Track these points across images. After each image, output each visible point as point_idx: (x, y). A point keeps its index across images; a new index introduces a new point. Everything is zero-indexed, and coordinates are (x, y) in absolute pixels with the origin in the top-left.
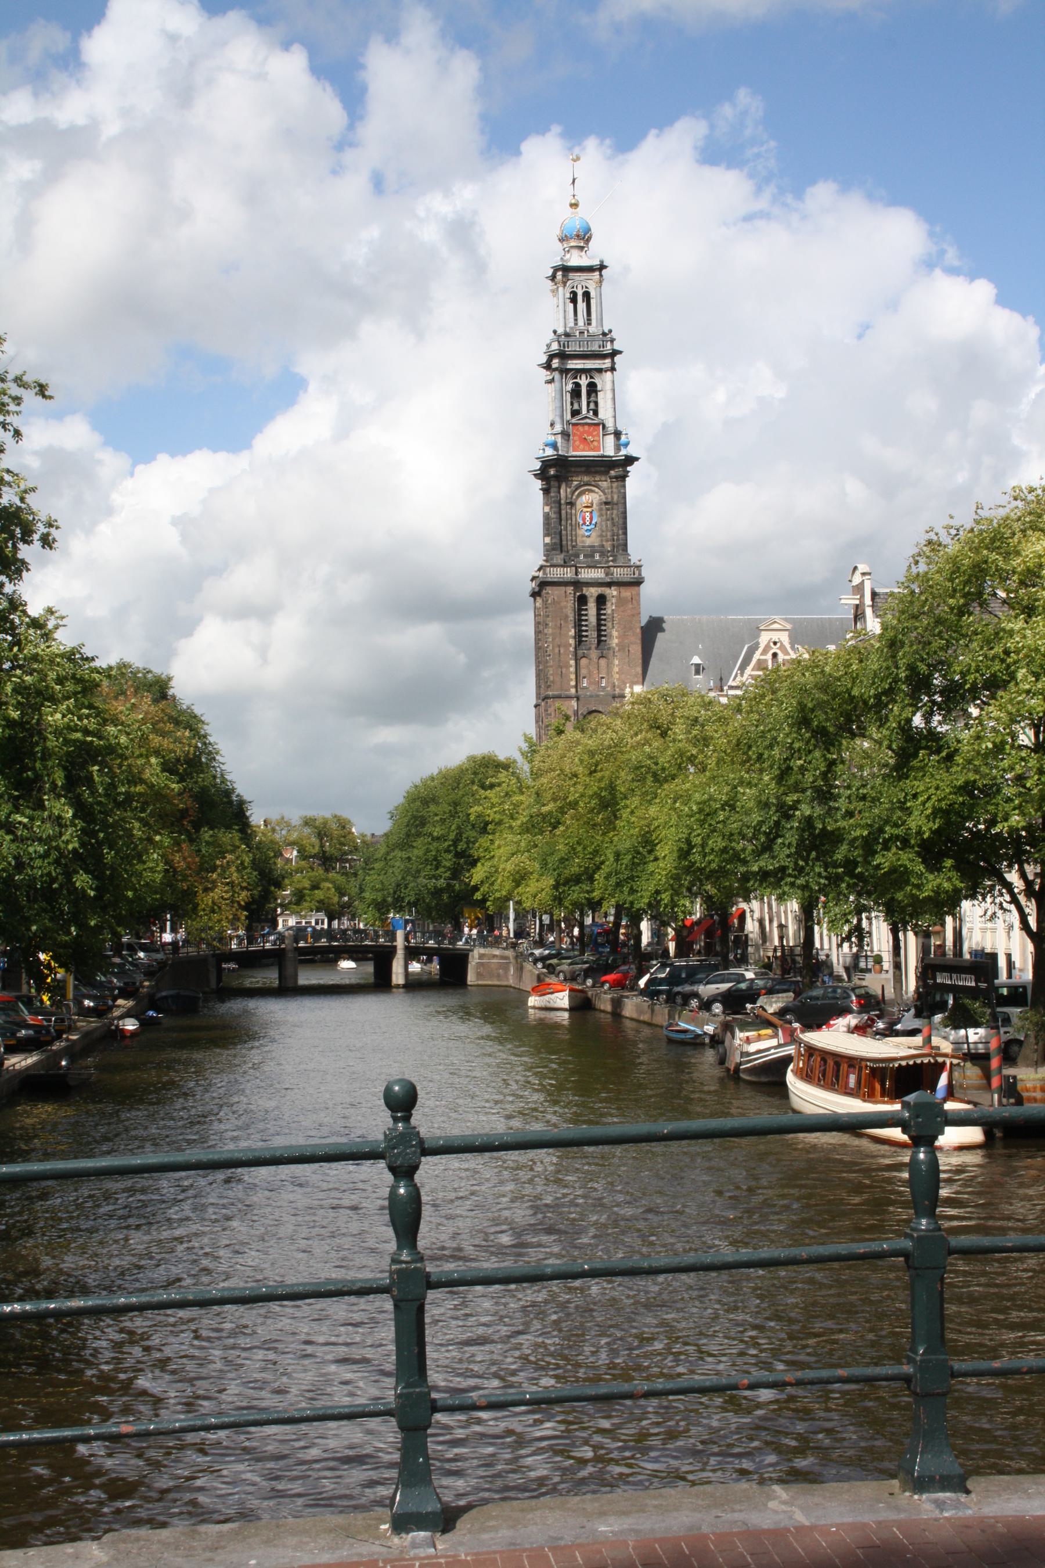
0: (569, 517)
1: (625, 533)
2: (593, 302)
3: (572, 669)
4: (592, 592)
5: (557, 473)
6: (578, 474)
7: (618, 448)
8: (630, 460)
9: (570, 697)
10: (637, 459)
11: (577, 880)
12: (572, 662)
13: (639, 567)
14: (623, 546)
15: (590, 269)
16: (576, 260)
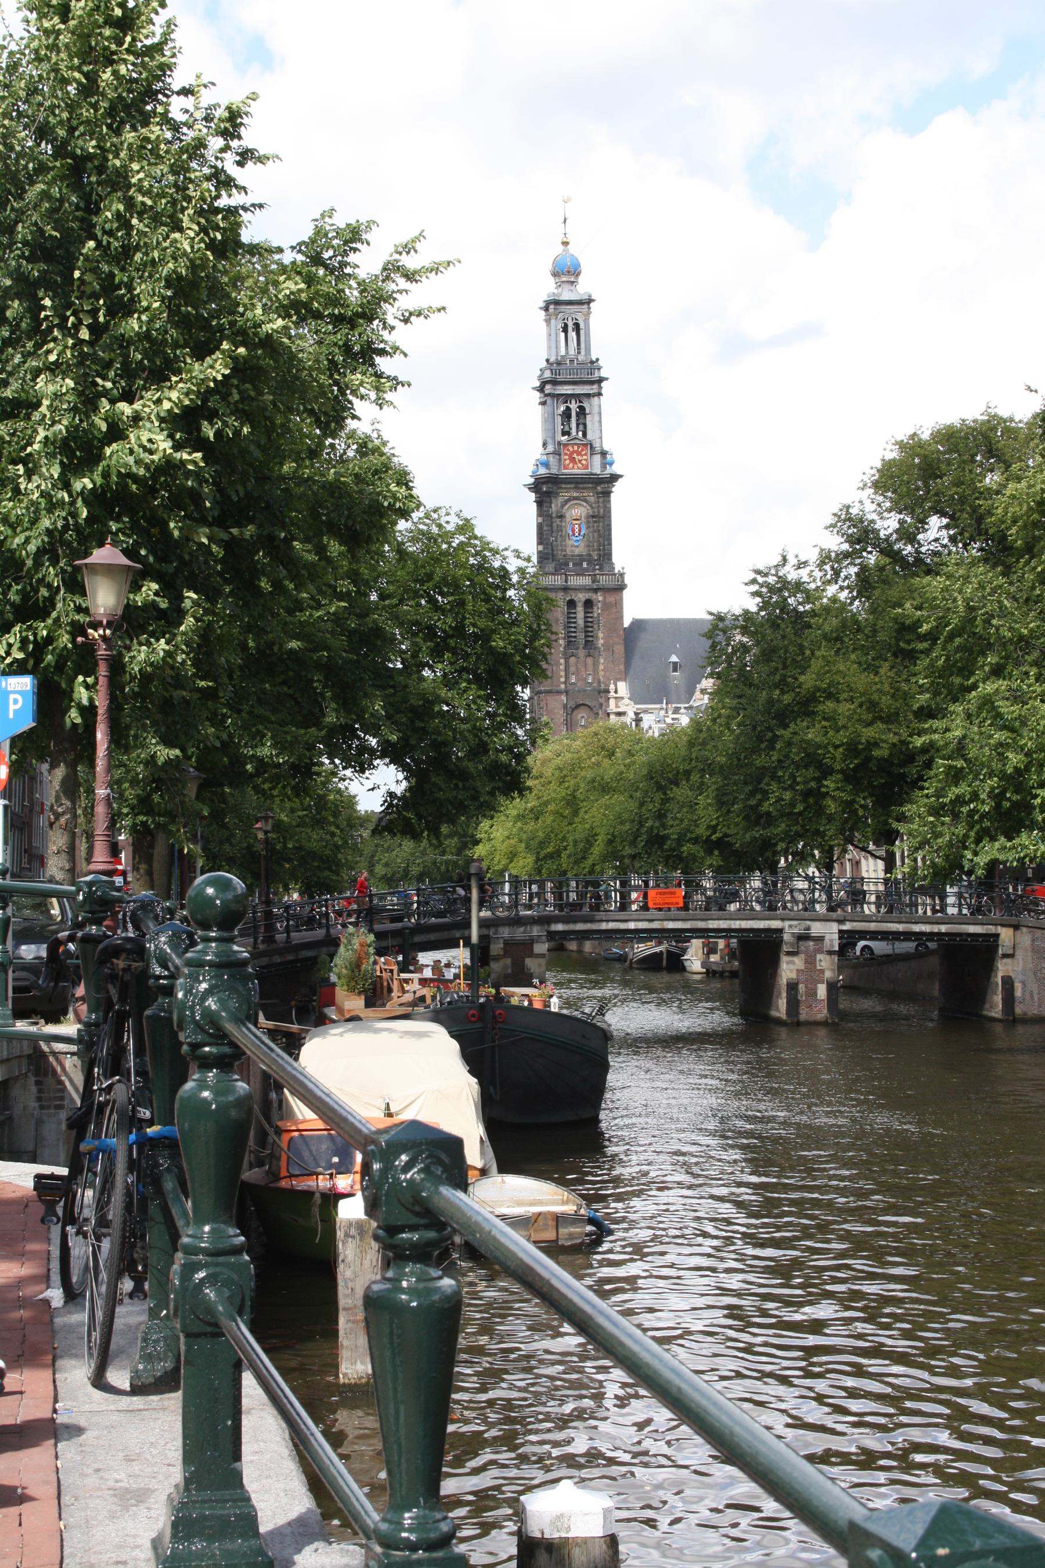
0: (560, 529)
1: (610, 544)
2: (582, 332)
3: (562, 667)
6: (567, 490)
7: (604, 466)
8: (615, 478)
9: (559, 692)
10: (621, 476)
11: (550, 856)
12: (562, 661)
13: (622, 575)
14: (606, 555)
15: (580, 303)
16: (566, 296)
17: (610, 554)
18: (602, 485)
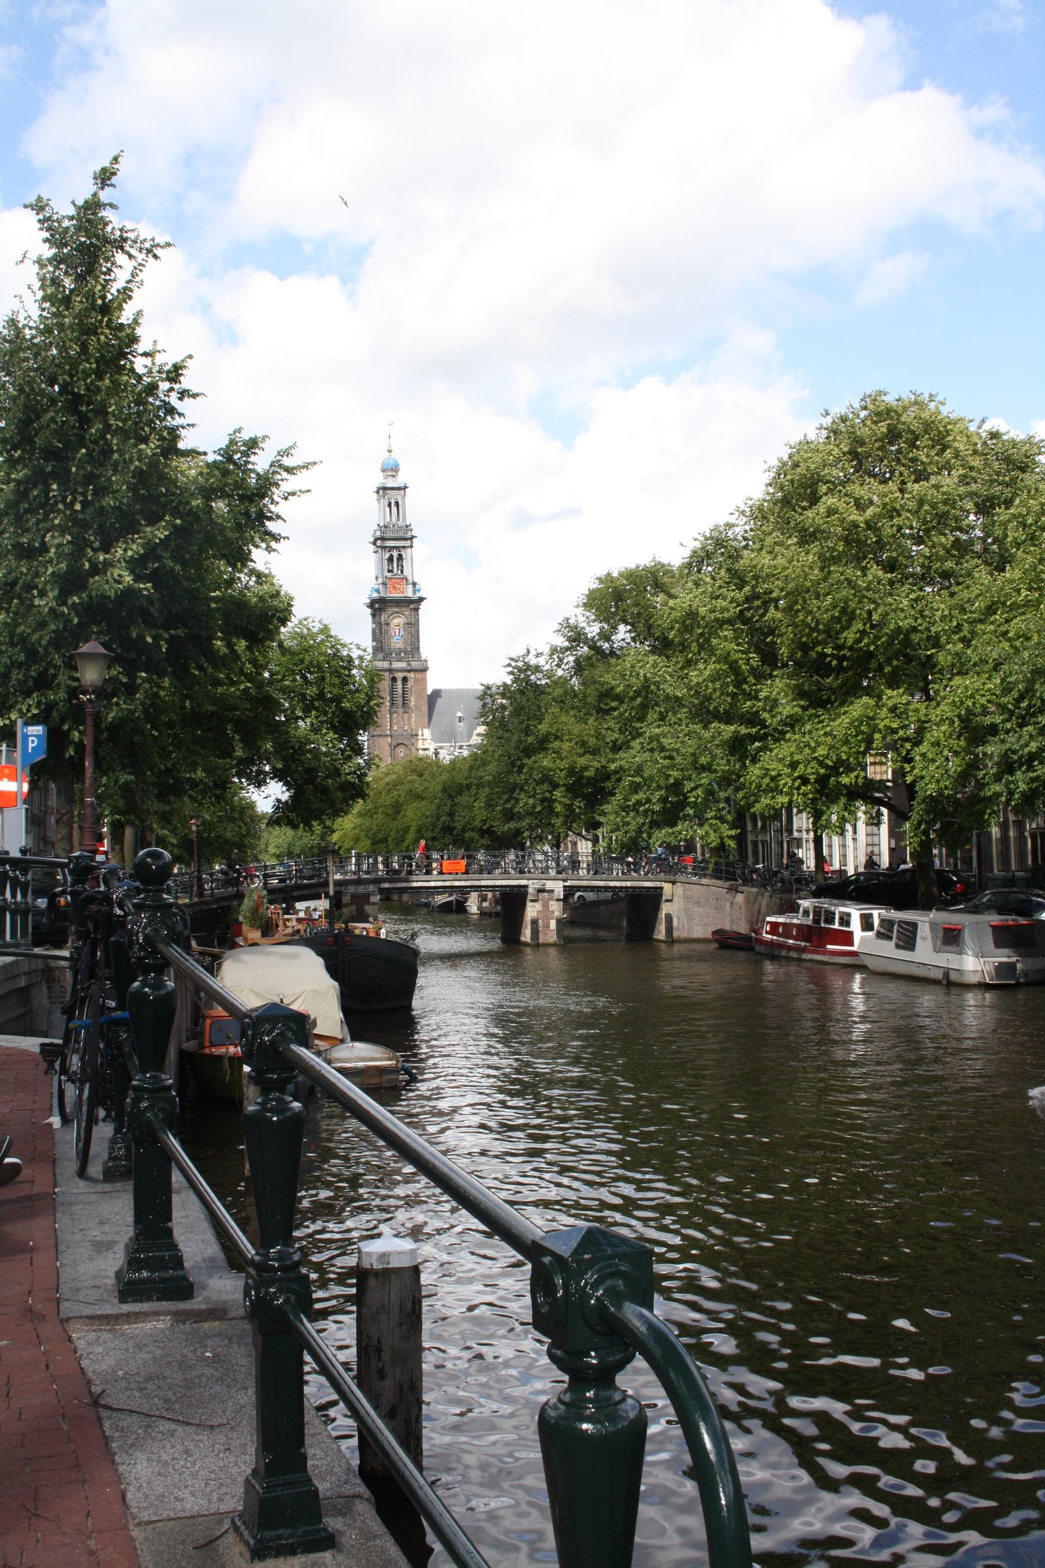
0: (387, 632)
4: (400, 675)
5: (378, 606)
7: (414, 592)
8: (421, 599)
14: (416, 648)
15: (399, 489)
17: (418, 648)
18: (413, 604)
